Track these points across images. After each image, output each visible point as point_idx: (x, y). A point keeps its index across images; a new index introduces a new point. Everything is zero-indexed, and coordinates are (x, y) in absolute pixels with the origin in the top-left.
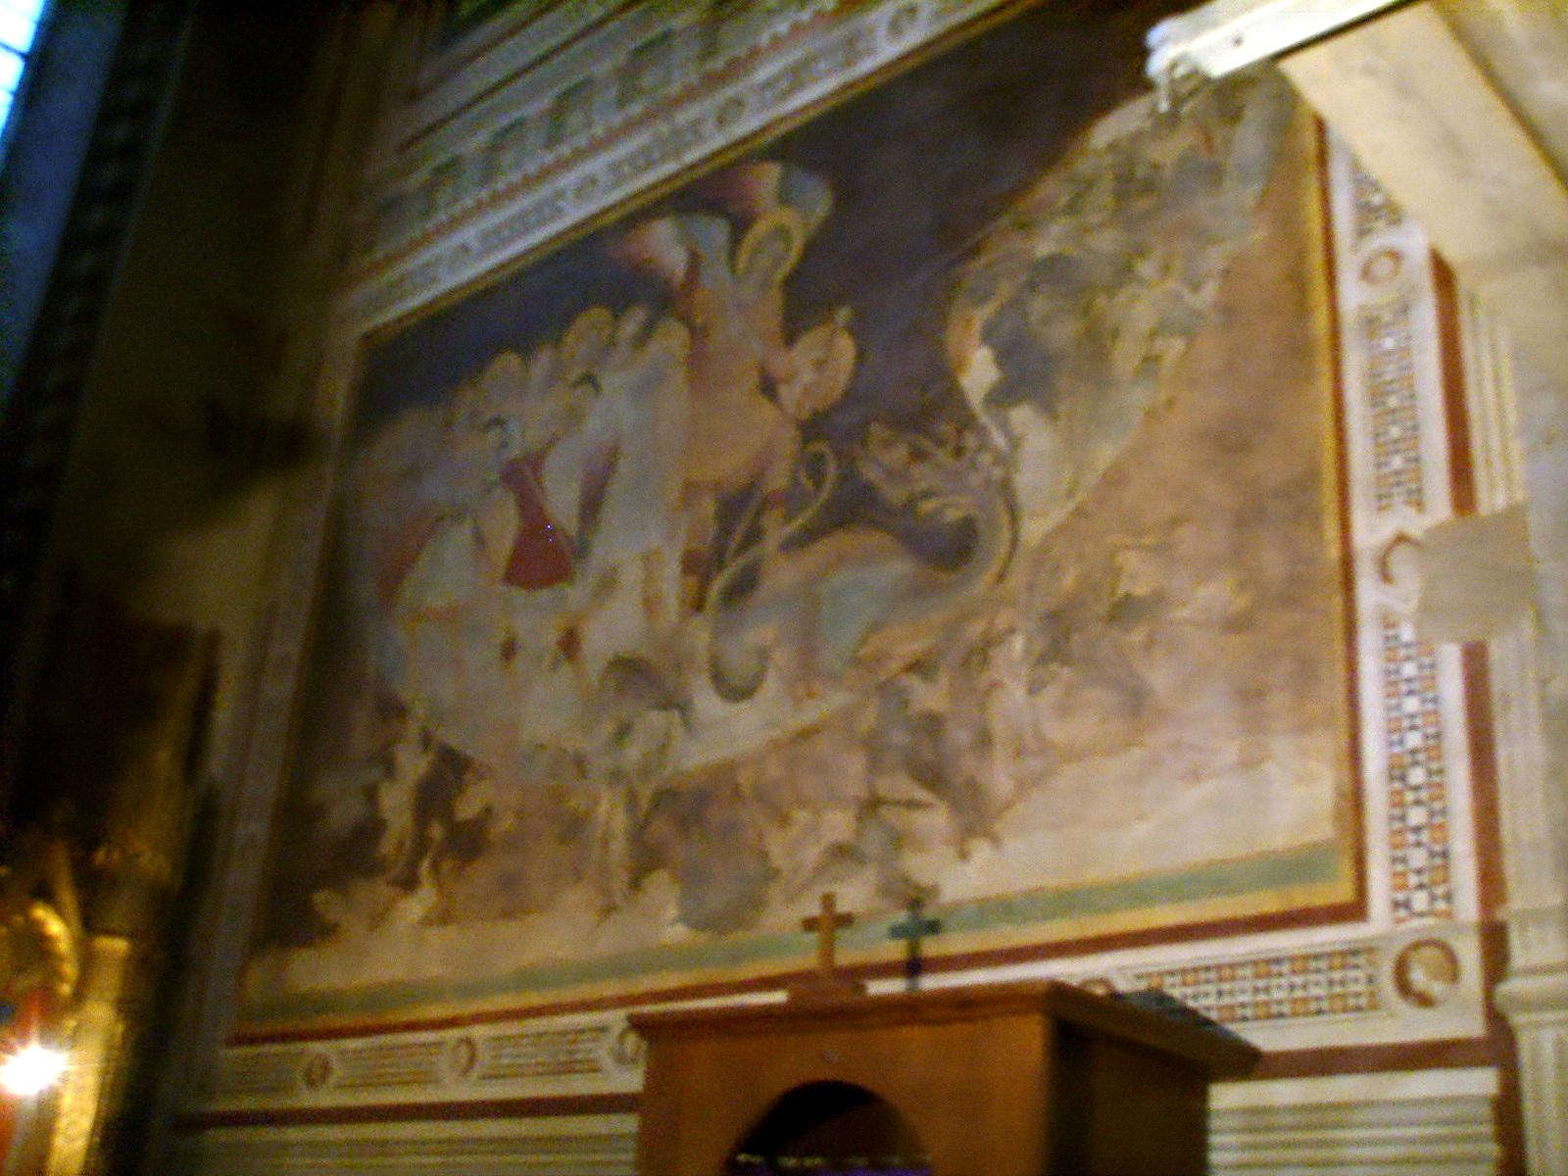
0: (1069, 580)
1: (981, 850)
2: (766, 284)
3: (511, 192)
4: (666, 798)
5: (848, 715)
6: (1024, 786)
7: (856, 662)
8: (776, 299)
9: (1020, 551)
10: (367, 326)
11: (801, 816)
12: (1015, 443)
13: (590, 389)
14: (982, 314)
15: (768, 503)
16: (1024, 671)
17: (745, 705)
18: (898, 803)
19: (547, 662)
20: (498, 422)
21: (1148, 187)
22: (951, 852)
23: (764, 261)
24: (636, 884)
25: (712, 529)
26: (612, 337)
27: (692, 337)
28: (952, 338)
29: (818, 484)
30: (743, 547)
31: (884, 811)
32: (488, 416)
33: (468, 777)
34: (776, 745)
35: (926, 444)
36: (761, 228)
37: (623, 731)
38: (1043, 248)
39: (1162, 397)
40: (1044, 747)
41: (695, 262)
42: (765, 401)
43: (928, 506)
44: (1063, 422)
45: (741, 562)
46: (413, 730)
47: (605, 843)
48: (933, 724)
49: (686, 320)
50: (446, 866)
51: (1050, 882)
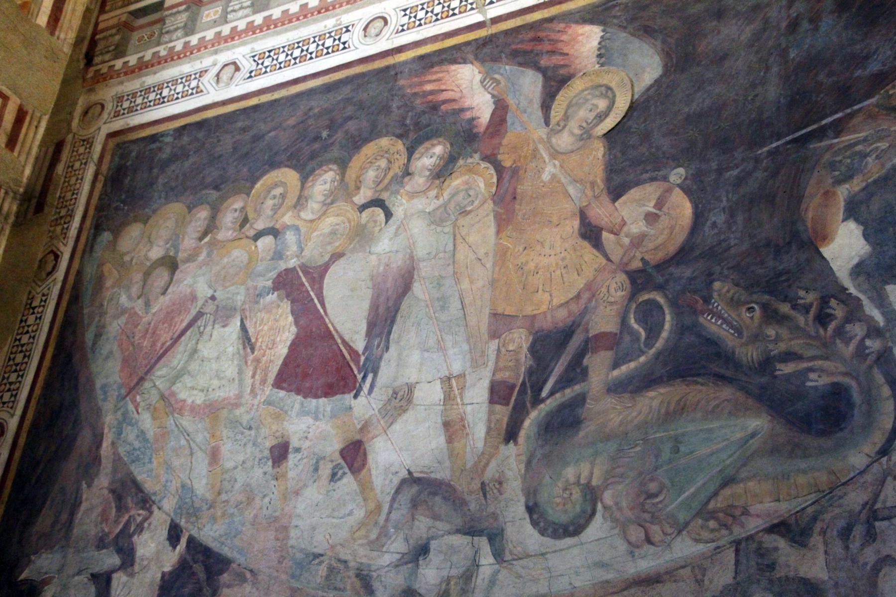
2: (586, 136)
3: (288, 19)
7: (704, 513)
8: (599, 150)
13: (379, 213)
17: (569, 541)
19: (326, 470)
20: (274, 232)
23: (584, 114)
25: (525, 360)
26: (407, 165)
27: (499, 180)
28: (810, 211)
29: (653, 332)
30: (565, 381)
32: (260, 225)
33: (225, 577)
35: (785, 308)
36: (577, 85)
37: (422, 550)
42: (586, 244)
43: (787, 368)
46: (159, 522)
49: (491, 159)
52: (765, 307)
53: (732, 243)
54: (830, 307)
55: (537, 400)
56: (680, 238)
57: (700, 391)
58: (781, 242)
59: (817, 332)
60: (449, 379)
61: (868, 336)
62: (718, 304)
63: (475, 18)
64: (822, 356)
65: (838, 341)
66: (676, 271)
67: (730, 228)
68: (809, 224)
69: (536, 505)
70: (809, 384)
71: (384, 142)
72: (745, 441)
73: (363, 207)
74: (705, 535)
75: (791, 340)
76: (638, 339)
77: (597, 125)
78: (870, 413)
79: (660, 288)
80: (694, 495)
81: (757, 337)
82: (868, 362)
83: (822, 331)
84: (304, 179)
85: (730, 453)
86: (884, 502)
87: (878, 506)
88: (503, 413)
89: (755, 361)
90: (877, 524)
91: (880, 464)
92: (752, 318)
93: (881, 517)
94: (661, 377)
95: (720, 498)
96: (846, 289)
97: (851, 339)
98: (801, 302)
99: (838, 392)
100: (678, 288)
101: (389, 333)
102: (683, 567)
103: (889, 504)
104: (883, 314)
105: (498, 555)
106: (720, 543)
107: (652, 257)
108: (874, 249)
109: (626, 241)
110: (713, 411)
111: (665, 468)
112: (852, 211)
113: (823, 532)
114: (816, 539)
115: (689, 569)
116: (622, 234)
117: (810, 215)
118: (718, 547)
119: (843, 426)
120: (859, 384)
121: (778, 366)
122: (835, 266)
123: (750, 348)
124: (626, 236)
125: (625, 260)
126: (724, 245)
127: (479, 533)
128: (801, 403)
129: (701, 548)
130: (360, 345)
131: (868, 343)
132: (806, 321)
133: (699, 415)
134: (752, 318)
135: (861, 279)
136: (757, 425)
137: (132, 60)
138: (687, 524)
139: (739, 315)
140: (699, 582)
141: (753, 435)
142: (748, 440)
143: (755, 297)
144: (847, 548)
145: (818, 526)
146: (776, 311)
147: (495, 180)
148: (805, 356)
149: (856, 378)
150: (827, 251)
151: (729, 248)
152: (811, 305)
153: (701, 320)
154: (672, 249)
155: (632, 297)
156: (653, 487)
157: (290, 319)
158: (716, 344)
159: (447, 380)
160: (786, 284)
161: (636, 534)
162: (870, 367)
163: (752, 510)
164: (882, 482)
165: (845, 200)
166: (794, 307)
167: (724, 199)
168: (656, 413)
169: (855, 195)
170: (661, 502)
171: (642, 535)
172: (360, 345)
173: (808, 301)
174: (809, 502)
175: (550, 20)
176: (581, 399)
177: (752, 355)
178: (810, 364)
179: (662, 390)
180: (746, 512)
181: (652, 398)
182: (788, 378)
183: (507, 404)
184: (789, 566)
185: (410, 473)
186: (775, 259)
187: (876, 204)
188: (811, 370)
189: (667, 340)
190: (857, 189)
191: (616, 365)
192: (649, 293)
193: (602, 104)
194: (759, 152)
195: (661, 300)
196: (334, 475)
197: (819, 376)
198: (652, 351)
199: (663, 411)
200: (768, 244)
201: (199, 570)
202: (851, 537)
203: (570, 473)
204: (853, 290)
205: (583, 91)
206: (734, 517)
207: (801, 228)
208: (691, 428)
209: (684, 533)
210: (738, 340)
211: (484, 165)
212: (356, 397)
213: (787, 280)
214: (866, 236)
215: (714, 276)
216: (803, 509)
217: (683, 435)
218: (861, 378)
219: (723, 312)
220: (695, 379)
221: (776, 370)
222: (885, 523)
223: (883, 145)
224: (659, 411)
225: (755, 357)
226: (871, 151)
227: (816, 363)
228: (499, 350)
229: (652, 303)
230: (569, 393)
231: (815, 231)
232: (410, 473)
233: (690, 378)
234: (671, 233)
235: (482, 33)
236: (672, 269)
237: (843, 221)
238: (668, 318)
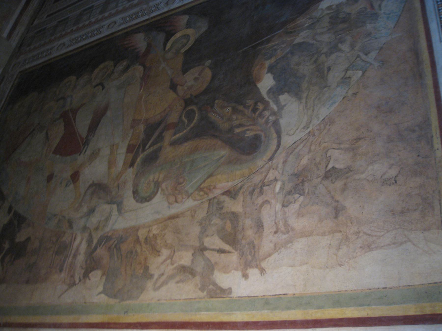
0: (304, 161)
1: (253, 272)
4: (106, 239)
5: (193, 211)
6: (277, 248)
7: (200, 189)
9: (281, 149)
10: (23, 68)
11: (165, 252)
12: (281, 108)
13: (100, 87)
14: (267, 63)
15: (167, 127)
16: (281, 197)
17: (146, 204)
18: (214, 250)
21: (344, 21)
22: (239, 274)
24: (86, 275)
25: (142, 136)
27: (144, 71)
29: (190, 120)
31: (207, 253)
34: (157, 222)
35: (241, 108)
36: (178, 35)
37: (92, 211)
38: (298, 40)
39: (350, 92)
40: (288, 229)
41: (149, 46)
44: (304, 101)
45: (152, 149)
46: (6, 205)
47: (75, 256)
48: (235, 216)
50: (7, 259)
51: (291, 291)
54: (258, 106)
55: (144, 150)
60: (113, 145)
61: (270, 115)
63: (147, 17)
69: (137, 190)
70: (246, 135)
71: (106, 63)
73: (95, 87)
74: (198, 197)
77: (182, 48)
80: (196, 182)
83: (253, 115)
84: (77, 79)
86: (268, 179)
87: (266, 181)
88: (131, 156)
90: (264, 188)
93: (266, 185)
95: (206, 182)
97: (264, 117)
98: (247, 105)
99: (257, 138)
101: (96, 130)
102: (188, 211)
103: (270, 179)
104: (278, 107)
105: (120, 211)
106: (203, 200)
109: (186, 88)
112: (271, 70)
113: (243, 193)
114: (240, 198)
115: (190, 211)
118: (202, 202)
121: (236, 130)
127: (114, 203)
129: (196, 203)
130: (84, 135)
131: (270, 118)
137: (32, 47)
138: (192, 194)
140: (193, 216)
144: (252, 198)
145: (242, 190)
147: (143, 71)
156: (181, 180)
157: (63, 128)
159: (112, 146)
161: (172, 199)
162: (270, 127)
163: (217, 186)
164: (268, 172)
170: (183, 186)
171: (174, 200)
172: (84, 135)
174: (240, 181)
175: (172, 15)
176: (160, 149)
177: (226, 126)
180: (215, 188)
183: (132, 153)
184: (228, 207)
185: (93, 181)
190: (273, 62)
191: (175, 134)
193: (185, 41)
194: (239, 52)
196: (66, 185)
198: (189, 128)
201: (16, 222)
202: (254, 194)
203: (151, 178)
204: (267, 99)
205: (179, 37)
206: (210, 190)
209: (190, 197)
211: (140, 67)
212: (80, 155)
216: (238, 184)
219: (218, 111)
222: (267, 187)
223: (284, 46)
225: (227, 127)
226: (279, 48)
228: (133, 133)
229: (193, 111)
230: (156, 147)
232: (93, 181)
235: (148, 22)
238: (197, 115)
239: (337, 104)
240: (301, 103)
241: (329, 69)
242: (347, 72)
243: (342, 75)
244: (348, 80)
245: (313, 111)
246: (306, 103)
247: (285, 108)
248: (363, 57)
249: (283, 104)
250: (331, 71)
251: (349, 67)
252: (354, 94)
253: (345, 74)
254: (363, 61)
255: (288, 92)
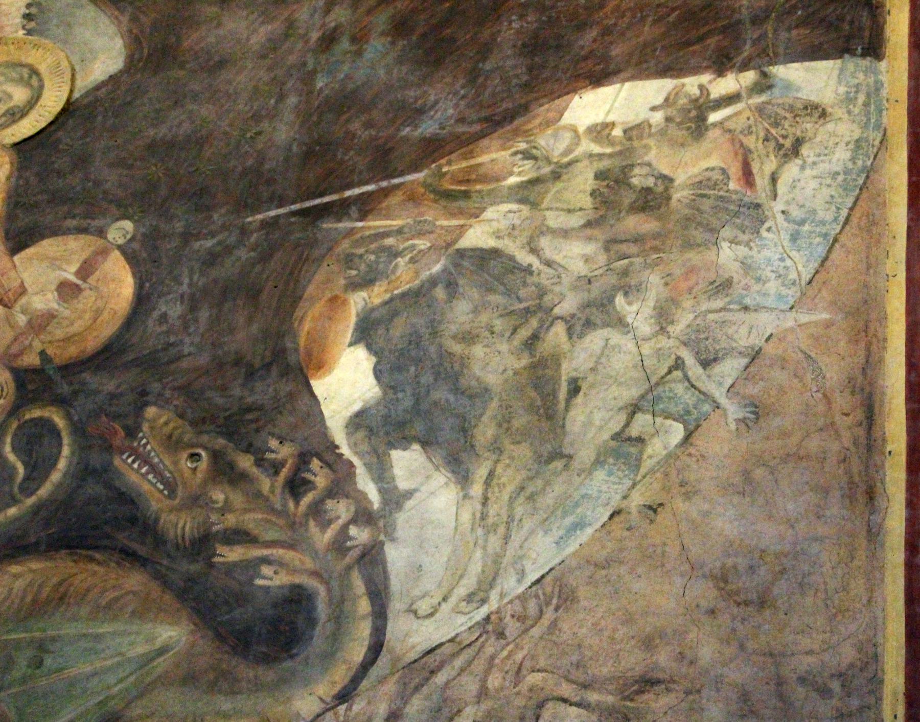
35: (245, 462)
39: (637, 499)
43: (232, 554)
44: (477, 489)
52: (216, 456)
53: (186, 351)
54: (309, 471)
56: (107, 329)
57: (95, 573)
58: (257, 363)
59: (285, 505)
62: (148, 443)
64: (285, 542)
65: (312, 523)
66: (91, 379)
67: (186, 327)
68: (302, 341)
72: (148, 660)
75: (246, 511)
76: (11, 477)
78: (337, 637)
79: (61, 402)
81: (196, 500)
82: (348, 560)
83: (291, 505)
85: (121, 675)
89: (187, 535)
91: (336, 714)
92: (194, 470)
94: (37, 544)
96: (337, 447)
97: (330, 522)
98: (268, 456)
100: (90, 406)
104: (381, 491)
107: (58, 352)
108: (385, 393)
110: (109, 606)
111: (14, 690)
116: (17, 307)
117: (307, 326)
119: (295, 651)
120: (329, 590)
121: (220, 549)
122: (327, 410)
123: (183, 515)
124: (24, 312)
125: (15, 349)
126: (173, 351)
128: (241, 610)
131: (353, 531)
132: (272, 486)
133: (84, 611)
134: (194, 470)
135: (361, 434)
136: (170, 637)
139: (176, 463)
141: (162, 651)
142: (152, 660)
143: (205, 438)
146: (231, 466)
148: (261, 540)
149: (327, 583)
150: (319, 386)
151: (179, 358)
152: (282, 464)
153: (117, 462)
154: (92, 344)
155: (15, 410)
158: (132, 502)
160: (254, 426)
165: (358, 315)
166: (260, 462)
167: (186, 281)
168: (17, 601)
169: (373, 310)
173: (279, 456)
177: (183, 528)
178: (265, 552)
179: (35, 565)
181: (16, 576)
182: (230, 569)
186: (243, 385)
187: (399, 329)
188: (266, 561)
189: (59, 485)
192: (43, 407)
195: (59, 421)
197: (276, 573)
199: (29, 599)
200: (237, 363)
204: (345, 451)
207: (289, 345)
208: (70, 630)
210: (168, 502)
213: (257, 420)
214: (378, 373)
215: (150, 398)
217: (54, 639)
218: (335, 584)
220: (90, 553)
221: (214, 555)
224: (23, 599)
227: (275, 551)
231: (309, 354)
233: (84, 552)
234: (95, 320)
236: (86, 376)
237: (350, 345)
239: (589, 531)
240: (466, 497)
241: (575, 389)
242: (634, 413)
243: (615, 426)
244: (633, 450)
245: (507, 538)
246: (485, 501)
247: (409, 504)
248: (695, 370)
249: (403, 484)
250: (580, 399)
251: (642, 397)
252: (650, 507)
253: (627, 425)
254: (693, 386)
255: (425, 444)
